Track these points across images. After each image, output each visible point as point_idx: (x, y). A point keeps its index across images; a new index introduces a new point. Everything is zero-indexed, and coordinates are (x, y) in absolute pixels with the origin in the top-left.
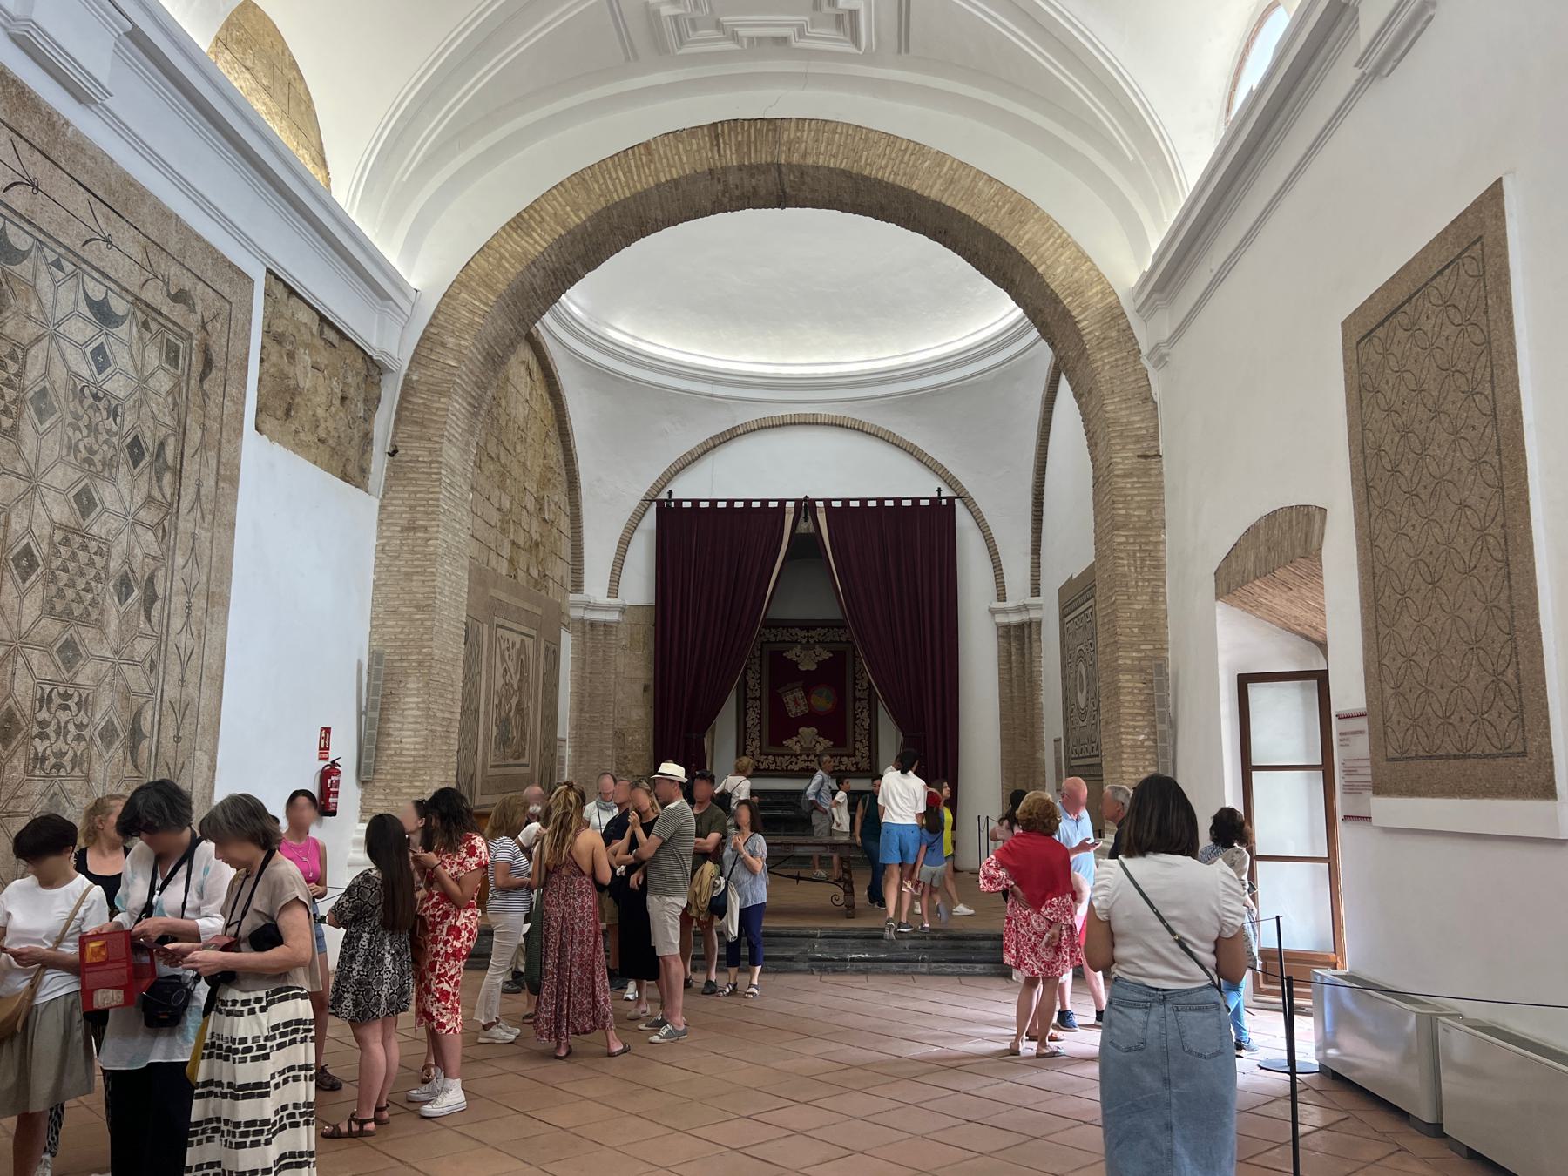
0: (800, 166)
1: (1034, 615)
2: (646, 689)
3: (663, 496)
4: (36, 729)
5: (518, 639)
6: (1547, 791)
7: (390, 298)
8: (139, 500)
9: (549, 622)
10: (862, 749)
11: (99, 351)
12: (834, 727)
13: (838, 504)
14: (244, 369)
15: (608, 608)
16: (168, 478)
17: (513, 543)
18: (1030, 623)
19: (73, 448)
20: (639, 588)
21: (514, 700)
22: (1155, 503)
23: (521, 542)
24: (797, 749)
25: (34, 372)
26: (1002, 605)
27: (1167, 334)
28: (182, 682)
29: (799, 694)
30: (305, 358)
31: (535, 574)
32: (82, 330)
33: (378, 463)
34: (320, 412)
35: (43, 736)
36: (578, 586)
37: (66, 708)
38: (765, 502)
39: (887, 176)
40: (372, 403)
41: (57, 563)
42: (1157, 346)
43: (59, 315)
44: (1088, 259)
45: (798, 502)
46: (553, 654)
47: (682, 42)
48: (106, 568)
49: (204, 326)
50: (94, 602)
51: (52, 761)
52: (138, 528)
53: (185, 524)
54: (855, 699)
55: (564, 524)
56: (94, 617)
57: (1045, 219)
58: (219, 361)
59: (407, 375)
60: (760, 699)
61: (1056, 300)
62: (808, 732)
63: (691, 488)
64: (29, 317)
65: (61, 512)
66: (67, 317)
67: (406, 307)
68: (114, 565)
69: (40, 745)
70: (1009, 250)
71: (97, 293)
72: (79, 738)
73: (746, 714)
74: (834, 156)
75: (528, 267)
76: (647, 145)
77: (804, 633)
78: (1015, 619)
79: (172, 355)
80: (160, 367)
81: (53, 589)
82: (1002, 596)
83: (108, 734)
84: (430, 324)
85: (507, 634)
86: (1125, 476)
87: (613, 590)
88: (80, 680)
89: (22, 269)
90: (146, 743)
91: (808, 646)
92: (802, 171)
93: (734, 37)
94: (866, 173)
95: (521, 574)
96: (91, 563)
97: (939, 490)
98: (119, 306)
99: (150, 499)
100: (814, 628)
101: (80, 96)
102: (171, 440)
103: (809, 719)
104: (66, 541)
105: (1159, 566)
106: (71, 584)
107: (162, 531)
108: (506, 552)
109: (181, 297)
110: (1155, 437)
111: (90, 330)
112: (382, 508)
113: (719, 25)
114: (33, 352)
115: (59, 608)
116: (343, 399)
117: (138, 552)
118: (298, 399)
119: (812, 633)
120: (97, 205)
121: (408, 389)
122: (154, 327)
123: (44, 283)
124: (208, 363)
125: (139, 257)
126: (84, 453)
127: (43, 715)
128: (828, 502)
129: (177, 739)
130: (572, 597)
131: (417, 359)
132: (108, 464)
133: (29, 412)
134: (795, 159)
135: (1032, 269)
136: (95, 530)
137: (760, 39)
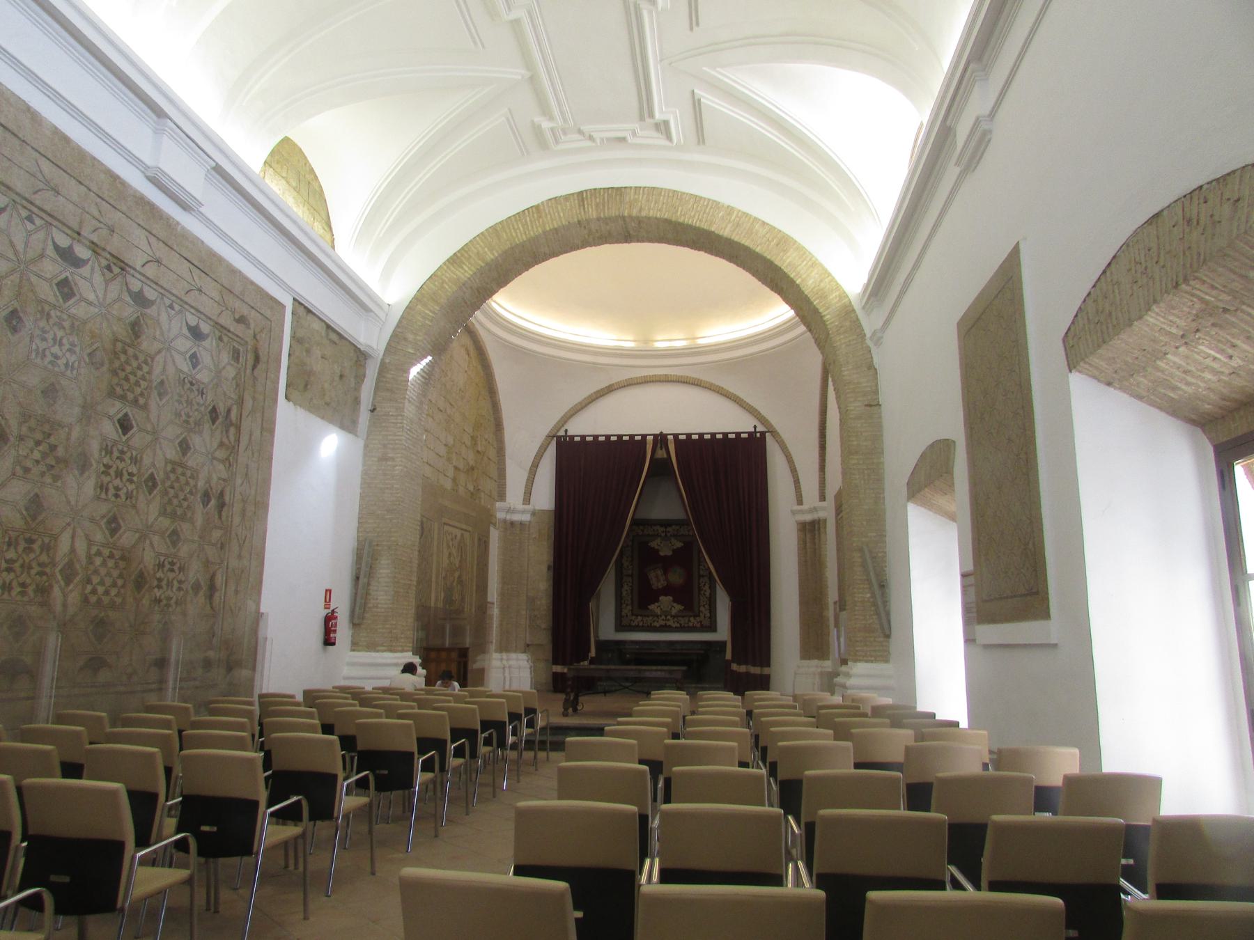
1: (821, 515)
2: (549, 568)
3: (562, 433)
4: (155, 583)
5: (459, 533)
8: (215, 445)
9: (484, 520)
10: (705, 611)
11: (194, 356)
12: (686, 596)
13: (683, 437)
14: (279, 361)
15: (523, 512)
16: (232, 430)
17: (456, 468)
18: (819, 521)
19: (178, 415)
20: (545, 497)
21: (457, 574)
23: (461, 467)
24: (658, 611)
25: (157, 369)
26: (799, 507)
28: (240, 557)
29: (659, 572)
30: (317, 352)
31: (471, 488)
32: (184, 344)
33: (364, 417)
34: (327, 386)
35: (159, 587)
36: (502, 496)
37: (172, 570)
38: (632, 436)
39: (695, 222)
40: (360, 378)
41: (168, 484)
42: (874, 333)
43: (172, 336)
44: (829, 274)
45: (655, 436)
46: (484, 544)
48: (195, 486)
49: (255, 337)
50: (189, 507)
51: (164, 602)
52: (215, 462)
53: (243, 458)
54: (700, 576)
55: (492, 453)
56: (189, 515)
58: (263, 358)
60: (632, 576)
62: (666, 600)
64: (155, 338)
65: (171, 453)
66: (176, 337)
67: (382, 315)
68: (201, 484)
69: (157, 593)
71: (193, 321)
72: (180, 589)
75: (460, 288)
76: (537, 207)
78: (808, 518)
79: (236, 355)
80: (229, 364)
81: (166, 498)
83: (196, 587)
84: (398, 326)
85: (451, 529)
87: (527, 499)
89: (152, 311)
90: (217, 594)
92: (639, 221)
93: (591, 138)
94: (681, 220)
95: (461, 489)
96: (187, 483)
98: (205, 328)
99: (221, 444)
100: (670, 525)
101: (185, 207)
102: (235, 407)
103: (667, 590)
104: (173, 471)
105: (879, 480)
106: (176, 496)
107: (228, 463)
108: (451, 473)
109: (241, 320)
110: (876, 392)
111: (189, 344)
112: (366, 446)
113: (580, 132)
115: (169, 509)
116: (341, 376)
118: (312, 378)
119: (669, 529)
120: (194, 270)
121: (383, 368)
122: (225, 339)
123: (164, 318)
124: (257, 359)
126: (184, 417)
127: (160, 574)
128: (676, 436)
129: (237, 592)
130: (498, 504)
131: (390, 348)
132: (198, 423)
133: (155, 394)
135: (792, 282)
136: (190, 463)
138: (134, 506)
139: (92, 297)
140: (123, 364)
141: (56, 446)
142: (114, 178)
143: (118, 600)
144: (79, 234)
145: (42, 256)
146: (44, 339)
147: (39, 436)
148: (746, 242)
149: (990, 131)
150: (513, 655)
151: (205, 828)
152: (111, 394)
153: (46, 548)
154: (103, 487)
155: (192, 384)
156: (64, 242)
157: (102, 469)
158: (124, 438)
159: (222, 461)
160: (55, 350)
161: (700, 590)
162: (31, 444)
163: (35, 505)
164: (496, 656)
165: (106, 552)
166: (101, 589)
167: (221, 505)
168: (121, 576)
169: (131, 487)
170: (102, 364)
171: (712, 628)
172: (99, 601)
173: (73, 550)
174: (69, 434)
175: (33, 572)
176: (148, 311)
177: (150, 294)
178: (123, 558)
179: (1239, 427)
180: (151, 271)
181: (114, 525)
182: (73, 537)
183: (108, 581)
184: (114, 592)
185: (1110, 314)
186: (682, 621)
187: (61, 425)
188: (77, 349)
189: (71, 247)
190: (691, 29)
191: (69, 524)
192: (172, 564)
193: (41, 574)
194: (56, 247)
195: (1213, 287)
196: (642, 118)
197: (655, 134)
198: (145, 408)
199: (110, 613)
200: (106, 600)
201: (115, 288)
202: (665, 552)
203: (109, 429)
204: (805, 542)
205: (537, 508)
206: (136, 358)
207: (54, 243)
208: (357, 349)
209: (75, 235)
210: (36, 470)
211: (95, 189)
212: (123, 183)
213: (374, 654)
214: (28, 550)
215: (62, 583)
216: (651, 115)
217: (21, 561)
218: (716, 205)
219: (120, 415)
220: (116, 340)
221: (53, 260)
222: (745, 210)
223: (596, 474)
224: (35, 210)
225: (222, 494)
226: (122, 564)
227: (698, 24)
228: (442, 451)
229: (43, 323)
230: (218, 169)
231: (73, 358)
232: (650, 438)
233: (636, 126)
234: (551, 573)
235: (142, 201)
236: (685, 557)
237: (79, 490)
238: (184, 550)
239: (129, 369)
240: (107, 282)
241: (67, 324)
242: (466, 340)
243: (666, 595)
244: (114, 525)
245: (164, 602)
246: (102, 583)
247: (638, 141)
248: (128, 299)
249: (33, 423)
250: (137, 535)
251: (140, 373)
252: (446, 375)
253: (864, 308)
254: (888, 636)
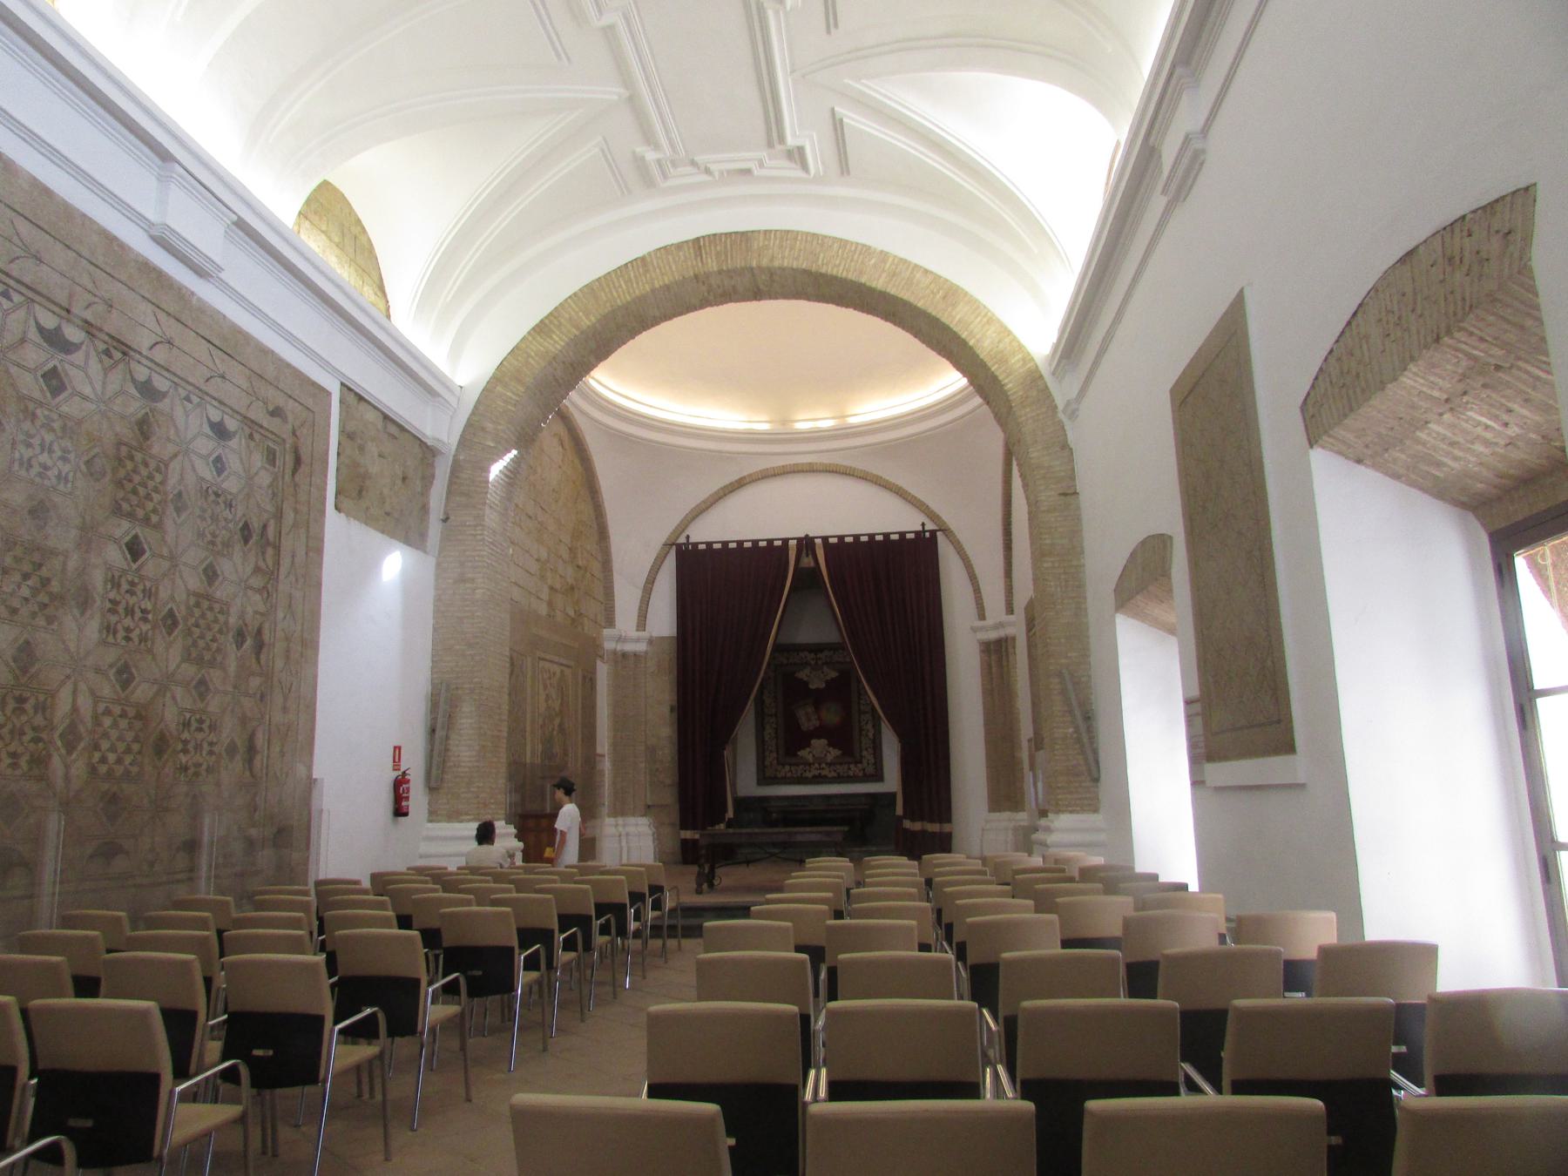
0: (769, 269)
1: (1009, 631)
2: (672, 709)
3: (682, 540)
4: (180, 746)
5: (557, 669)
6: (1289, 748)
7: (439, 395)
8: (249, 570)
9: (588, 652)
10: (868, 756)
11: (218, 459)
12: (842, 737)
13: (834, 540)
14: (326, 462)
15: (638, 640)
16: (270, 551)
19: (201, 535)
20: (664, 621)
21: (557, 721)
23: (558, 586)
24: (810, 758)
25: (173, 480)
26: (982, 623)
28: (285, 710)
29: (810, 709)
30: (372, 449)
31: (571, 613)
32: (206, 445)
33: (435, 529)
34: (386, 491)
35: (185, 751)
36: (610, 622)
38: (770, 542)
39: (840, 272)
40: (428, 480)
42: (1068, 404)
43: (189, 436)
45: (799, 540)
46: (590, 681)
47: (665, 177)
48: (226, 623)
49: (294, 433)
50: (219, 650)
52: (250, 592)
53: (283, 587)
55: (596, 567)
56: (219, 658)
58: (305, 457)
63: (707, 532)
64: (168, 439)
65: (195, 582)
66: (194, 438)
68: (232, 620)
69: (183, 758)
70: (945, 328)
71: (215, 416)
72: (211, 753)
74: (797, 259)
75: (550, 363)
76: (643, 259)
78: (993, 635)
79: (271, 457)
81: (190, 641)
83: (232, 750)
84: (473, 413)
85: (547, 665)
88: (210, 709)
89: (163, 406)
90: (258, 757)
92: (771, 272)
93: (708, 171)
94: (823, 271)
96: (216, 621)
98: (231, 424)
99: (257, 570)
103: (820, 732)
104: (198, 605)
105: (1080, 586)
106: (202, 637)
108: (545, 595)
109: (276, 413)
110: (1072, 478)
111: (211, 445)
112: (438, 565)
113: (693, 163)
114: (171, 466)
115: (194, 655)
116: (404, 479)
117: (250, 610)
120: (215, 352)
122: (257, 437)
123: (179, 413)
124: (298, 461)
125: (245, 385)
126: (209, 537)
127: (186, 735)
128: (825, 539)
129: (282, 754)
130: (606, 632)
131: (464, 442)
132: (227, 545)
133: (170, 510)
134: (765, 262)
135: (964, 343)
136: (218, 594)
137: (729, 172)
138: (150, 651)
139: (87, 391)
140: (130, 473)
141: (48, 580)
142: (110, 239)
143: (135, 770)
144: (68, 311)
145: (23, 341)
146: (29, 445)
147: (27, 567)
148: (905, 295)
149: (1203, 151)
150: (631, 820)
151: (258, 1052)
152: (117, 511)
153: (41, 708)
154: (109, 629)
155: (217, 495)
156: (49, 322)
157: (109, 605)
158: (135, 566)
159: (259, 591)
160: (44, 458)
161: (861, 730)
162: (17, 577)
163: (26, 655)
164: (609, 821)
165: (117, 710)
166: (112, 757)
167: (259, 646)
168: (136, 739)
169: (145, 627)
170: (104, 475)
171: (878, 776)
172: (110, 773)
173: (75, 709)
174: (65, 564)
175: (26, 738)
176: (160, 405)
177: (161, 383)
178: (138, 716)
179: (1520, 510)
180: (160, 355)
181: (125, 676)
182: (75, 692)
183: (121, 747)
184: (128, 759)
185: (1358, 375)
186: (841, 769)
187: (53, 553)
188: (72, 456)
189: (58, 329)
190: (829, 32)
191: (68, 677)
192: (201, 721)
193: (36, 740)
194: (41, 329)
195: (1482, 339)
196: (770, 145)
197: (785, 163)
198: (158, 527)
199: (124, 786)
200: (119, 770)
201: (116, 378)
202: (817, 684)
203: (115, 556)
204: (990, 666)
205: (655, 634)
206: (146, 465)
207: (37, 323)
208: (422, 444)
209: (64, 313)
210: (25, 611)
211: (85, 253)
212: (123, 246)
213: (457, 825)
214: (19, 710)
215: (63, 751)
216: (782, 139)
217: (9, 726)
218: (866, 250)
219: (127, 539)
220: (120, 444)
221: (39, 346)
222: (902, 255)
223: (727, 591)
224: (12, 283)
225: (259, 632)
226: (138, 724)
227: (836, 25)
228: (534, 567)
229: (27, 425)
230: (241, 224)
231: (66, 468)
232: (793, 543)
233: (763, 154)
234: (675, 715)
235: (147, 268)
236: (841, 689)
237: (81, 632)
238: (214, 705)
239: (137, 479)
240: (106, 371)
241: (56, 425)
242: (560, 428)
243: (819, 737)
244: (125, 676)
245: (191, 771)
246: (113, 749)
247: (764, 172)
248: (134, 391)
249: (18, 551)
250: (156, 687)
251: (151, 484)
252: (535, 472)
254: (1096, 780)
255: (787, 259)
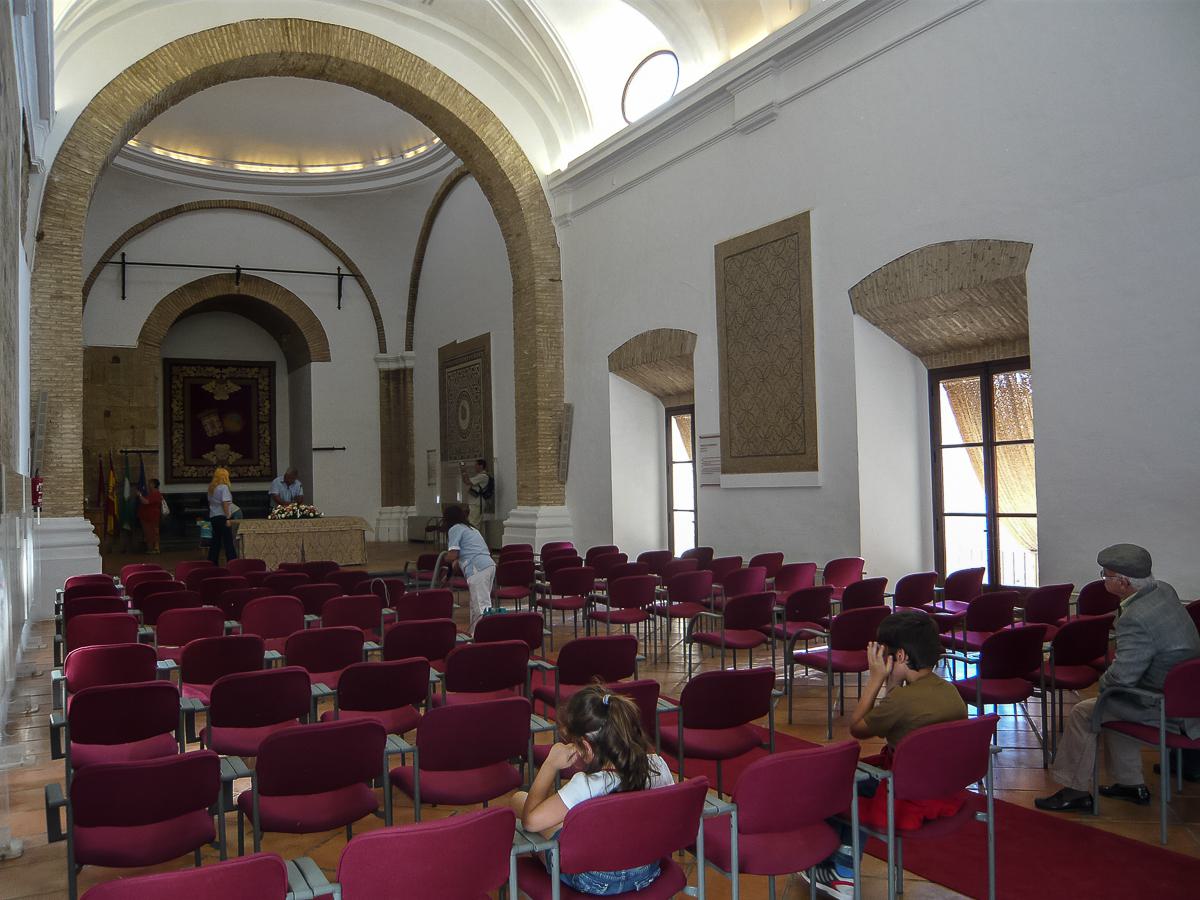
1: (409, 364)
22: (558, 309)
26: (383, 355)
27: (570, 209)
29: (215, 418)
39: (402, 77)
44: (523, 153)
54: (259, 422)
57: (499, 123)
59: (49, 177)
60: (183, 422)
61: (503, 175)
73: (172, 434)
74: (369, 58)
76: (236, 25)
77: (218, 370)
78: (393, 366)
82: (383, 350)
84: (68, 138)
86: (541, 291)
91: (222, 381)
92: (343, 63)
94: (389, 73)
97: (339, 269)
100: (226, 367)
103: (224, 438)
119: (224, 371)
121: (50, 189)
134: (342, 55)
179: (949, 362)
195: (982, 294)
204: (388, 390)
253: (551, 190)
255: (362, 57)
